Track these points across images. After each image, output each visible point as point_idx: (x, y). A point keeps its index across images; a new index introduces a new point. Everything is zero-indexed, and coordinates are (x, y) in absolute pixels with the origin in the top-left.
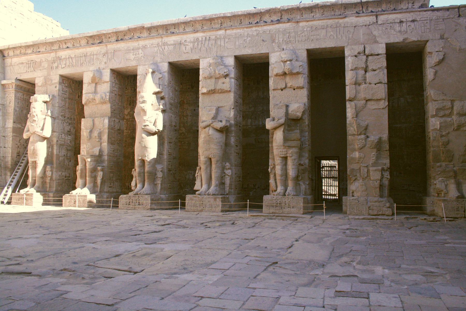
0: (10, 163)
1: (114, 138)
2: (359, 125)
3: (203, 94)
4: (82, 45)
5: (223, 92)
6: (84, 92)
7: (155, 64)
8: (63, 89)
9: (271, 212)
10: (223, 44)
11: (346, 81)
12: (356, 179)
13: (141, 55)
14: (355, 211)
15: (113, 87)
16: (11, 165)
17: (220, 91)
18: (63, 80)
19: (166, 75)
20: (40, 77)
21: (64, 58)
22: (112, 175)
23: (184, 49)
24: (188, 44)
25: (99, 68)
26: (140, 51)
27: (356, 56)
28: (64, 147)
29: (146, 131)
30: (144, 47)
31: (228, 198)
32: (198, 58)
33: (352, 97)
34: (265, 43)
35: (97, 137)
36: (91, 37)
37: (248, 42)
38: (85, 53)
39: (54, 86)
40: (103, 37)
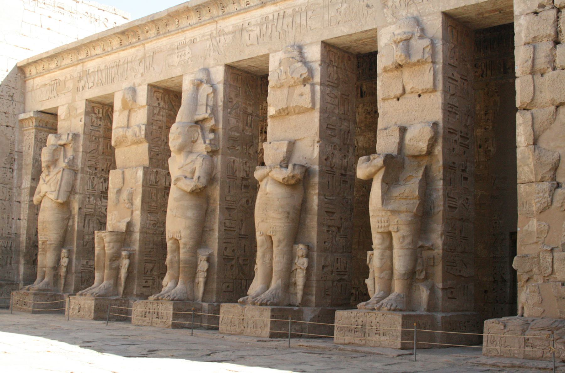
0: (25, 245)
1: (156, 202)
2: (539, 162)
3: (272, 117)
4: (114, 48)
5: (302, 111)
6: (114, 126)
7: (207, 71)
8: (92, 123)
9: (347, 342)
10: (304, 22)
11: (516, 68)
12: (528, 280)
13: (188, 56)
14: (498, 348)
15: (154, 115)
16: (27, 247)
17: (297, 111)
18: (93, 108)
19: (220, 88)
20: (63, 105)
21: (93, 72)
22: (149, 266)
23: (247, 38)
24: (252, 28)
25: (134, 84)
26: (187, 49)
27: (536, 13)
28: (95, 218)
29: (180, 188)
30: (193, 41)
31: (300, 312)
32: (267, 52)
33: (527, 100)
34: (370, 11)
35: (126, 201)
36: (123, 33)
37: (343, 12)
38: (118, 61)
39: (79, 119)
40: (140, 32)
